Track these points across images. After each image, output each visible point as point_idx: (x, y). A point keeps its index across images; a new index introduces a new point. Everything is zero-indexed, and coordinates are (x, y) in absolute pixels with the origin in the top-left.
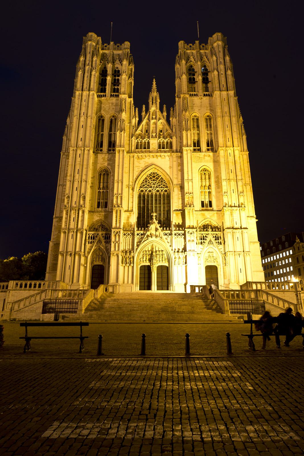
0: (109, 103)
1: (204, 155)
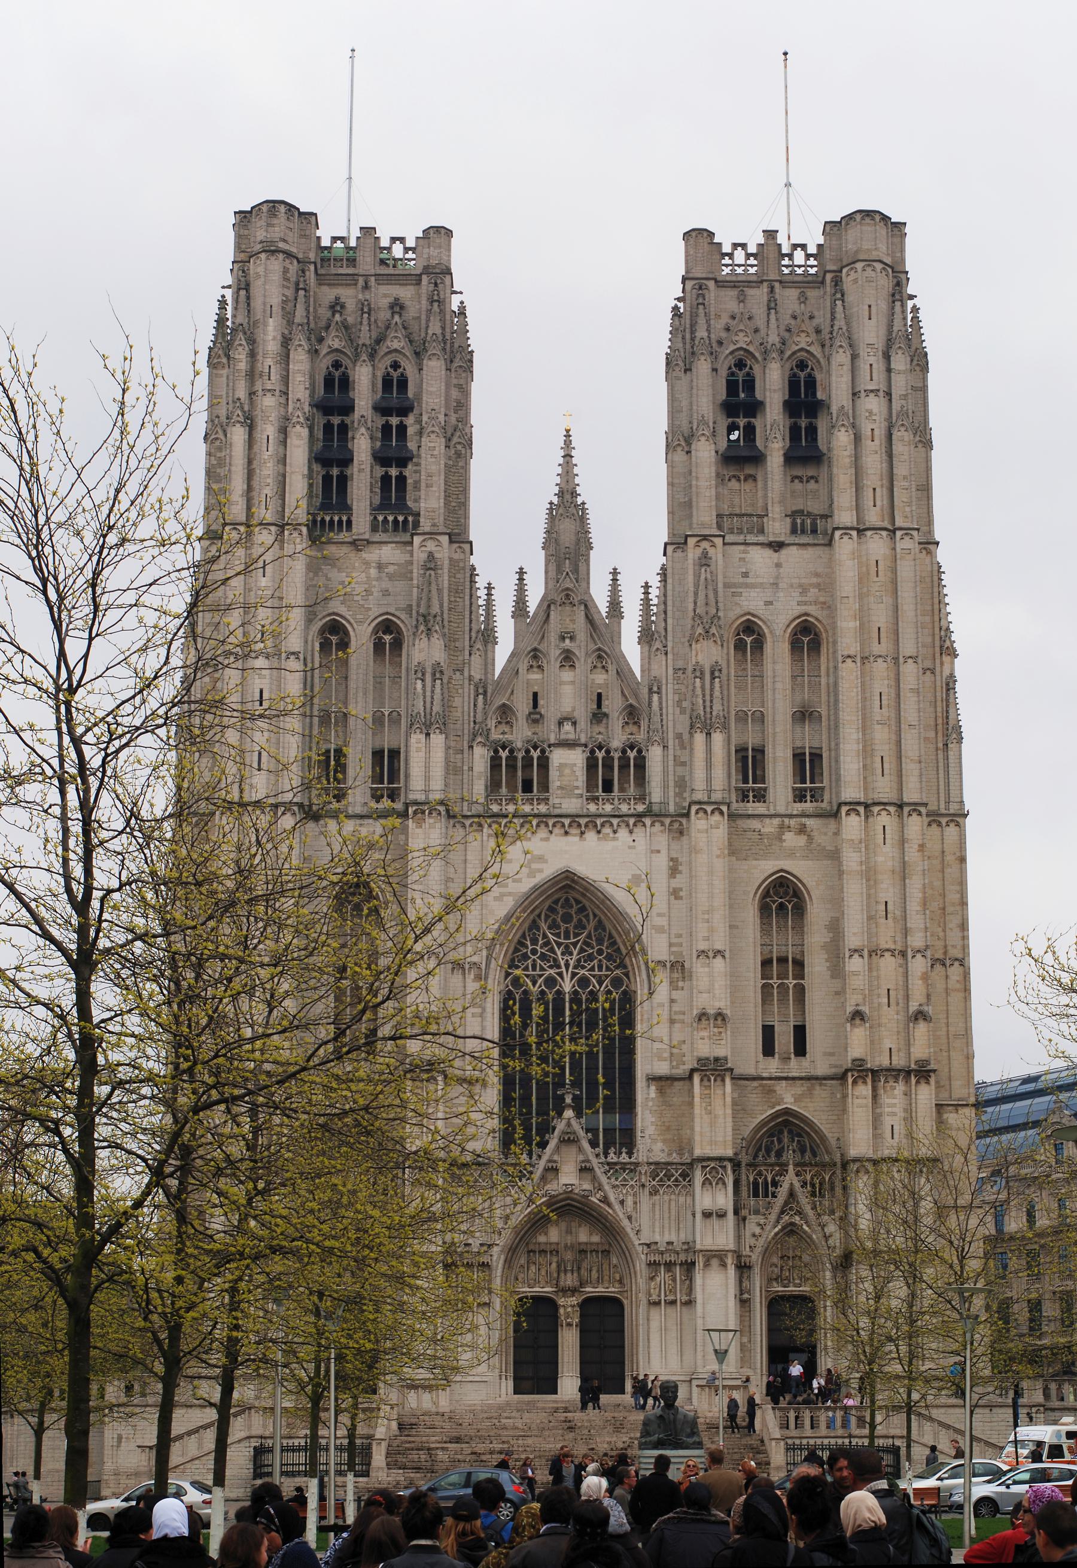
0: (367, 564)
1: (782, 827)
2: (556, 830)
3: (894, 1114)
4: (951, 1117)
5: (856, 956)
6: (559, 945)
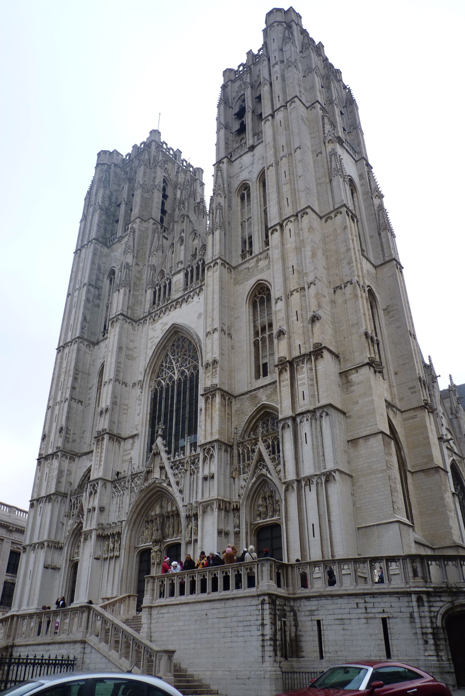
2: (172, 309)
3: (304, 384)
4: (354, 377)
5: (279, 301)
6: (174, 359)
